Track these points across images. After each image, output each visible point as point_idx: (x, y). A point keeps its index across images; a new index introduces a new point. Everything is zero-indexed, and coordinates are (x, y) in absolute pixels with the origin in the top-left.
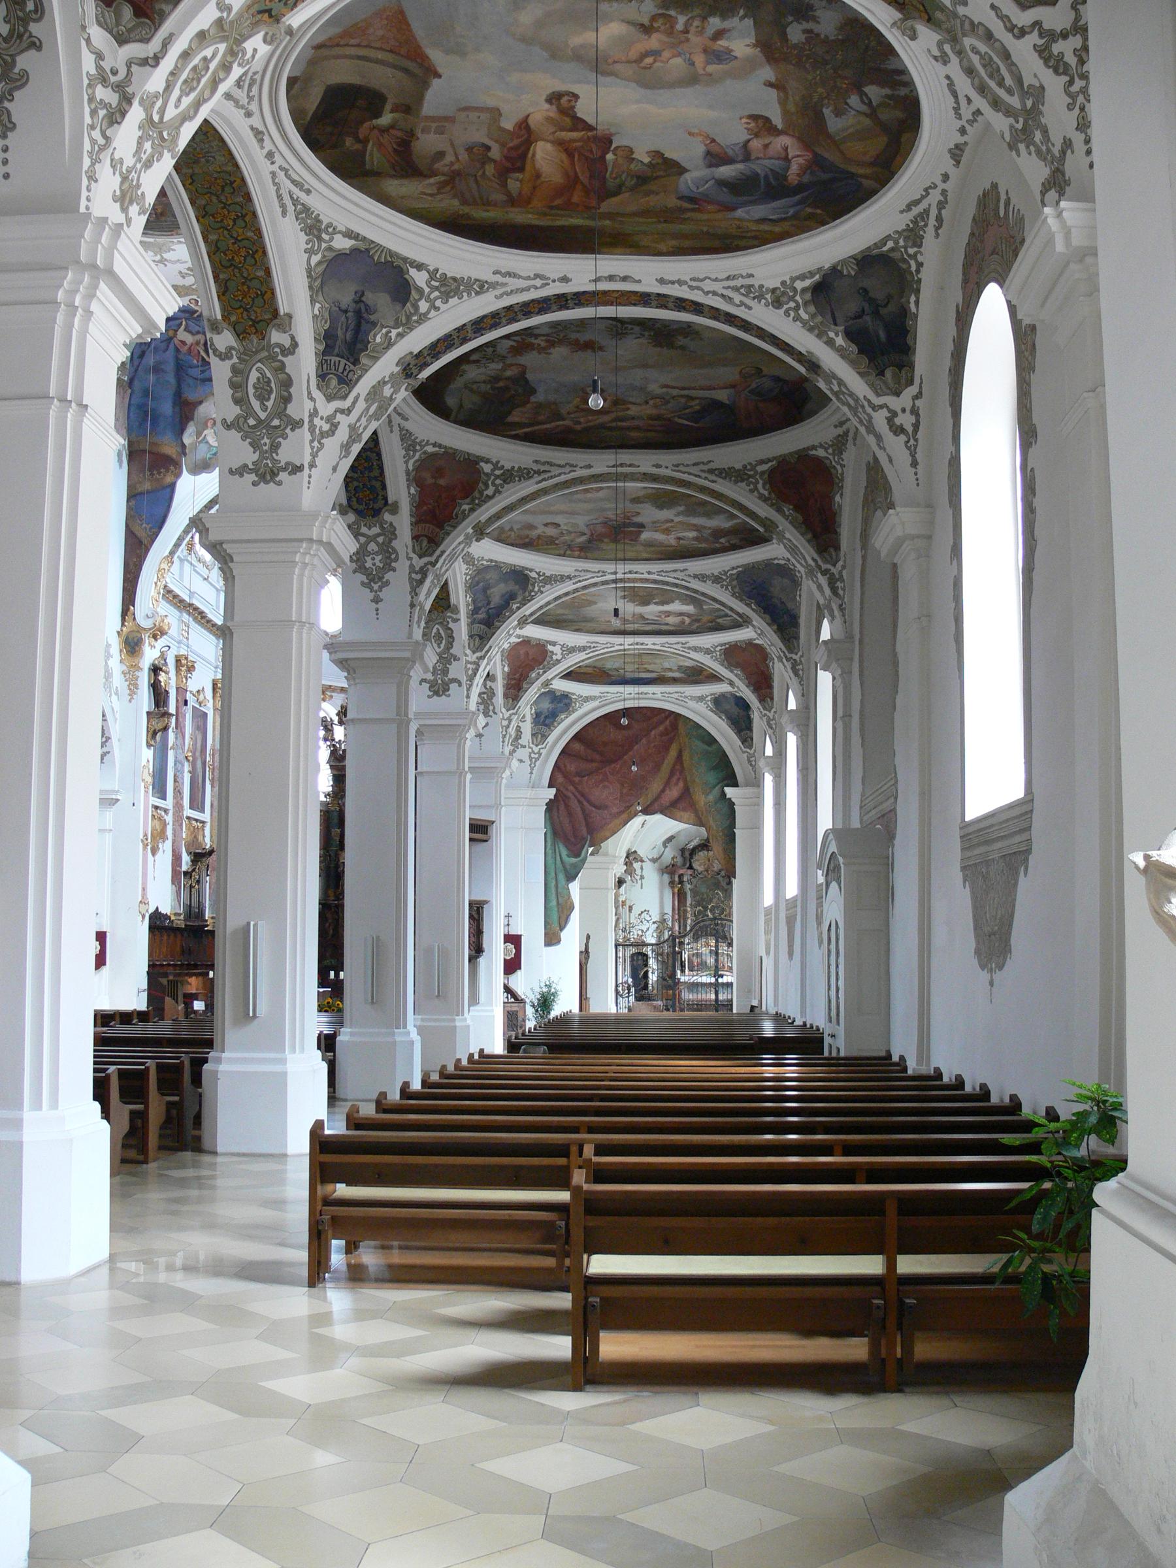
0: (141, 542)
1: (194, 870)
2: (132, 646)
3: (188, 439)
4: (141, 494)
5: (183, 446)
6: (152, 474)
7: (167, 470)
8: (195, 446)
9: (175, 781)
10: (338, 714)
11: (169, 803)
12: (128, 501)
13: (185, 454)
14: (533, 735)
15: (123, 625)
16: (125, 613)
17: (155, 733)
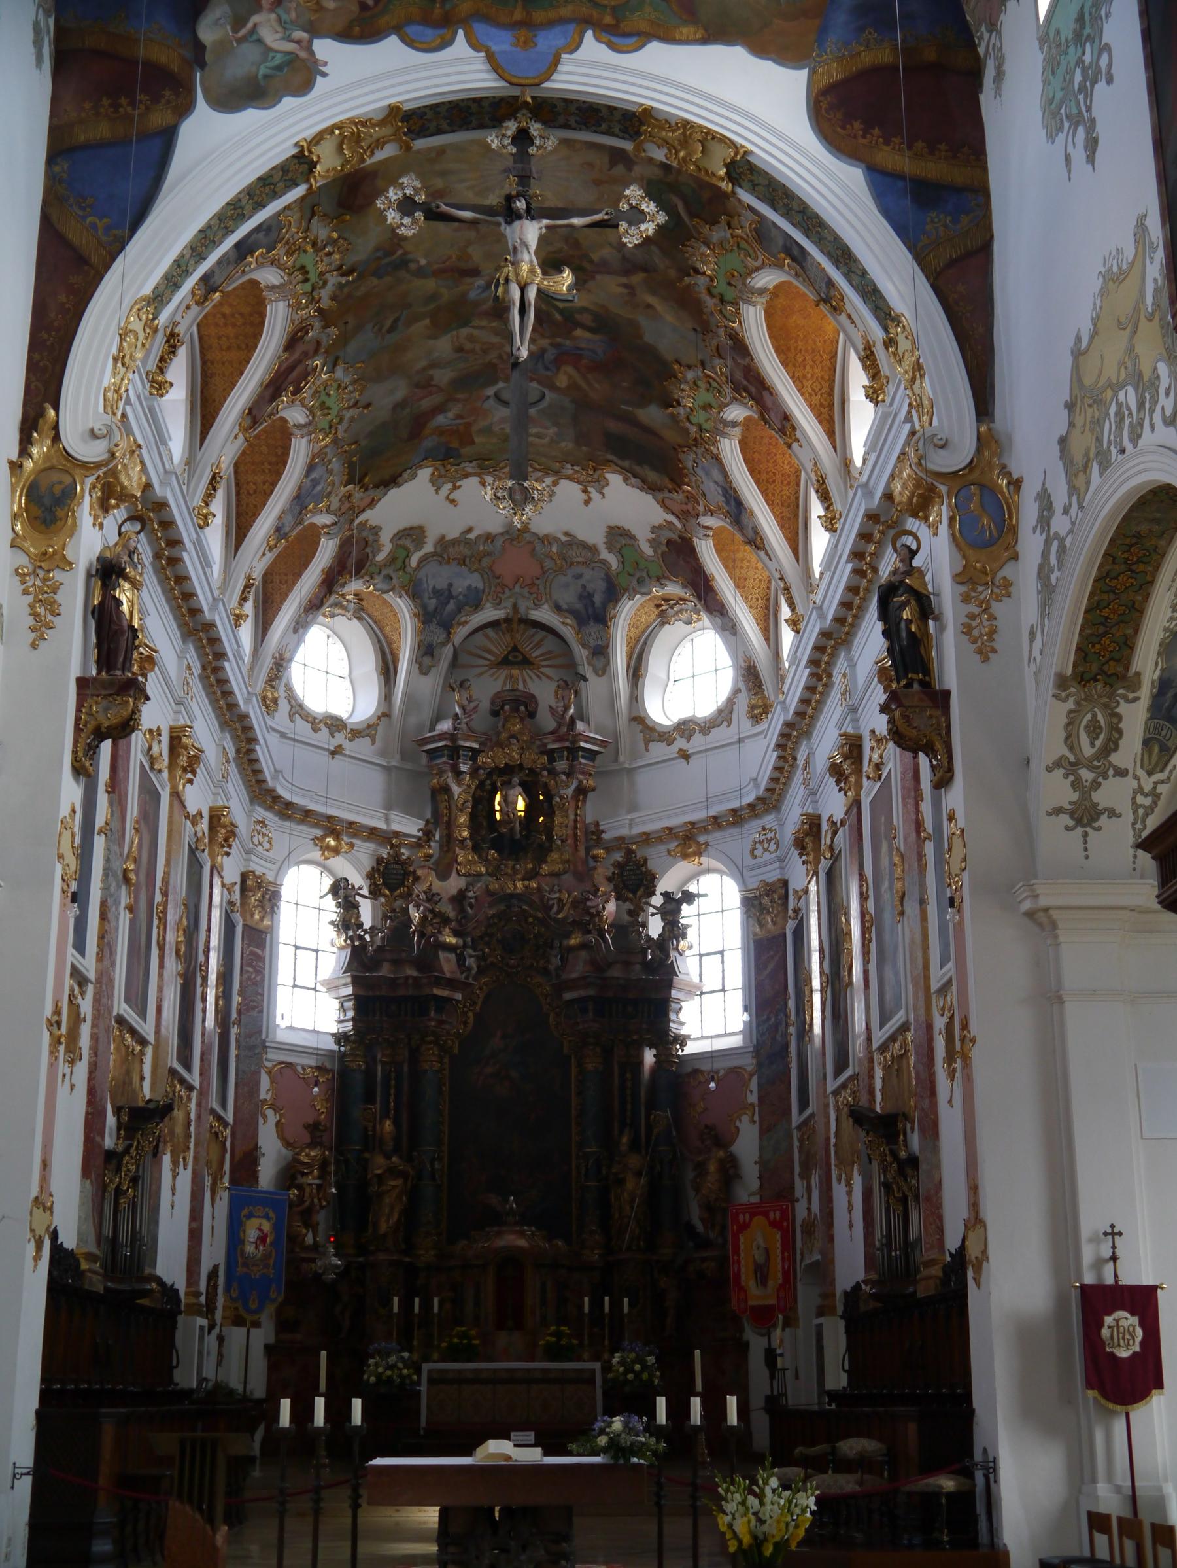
0: (81, 260)
1: (127, 1150)
2: (46, 507)
3: (209, 32)
4: (85, 147)
5: (199, 47)
6: (116, 106)
7: (156, 99)
8: (224, 47)
9: (103, 917)
10: (370, 876)
11: (89, 965)
12: (51, 160)
13: (202, 65)
14: (1146, 743)
15: (24, 452)
16: (30, 425)
17: (100, 735)
